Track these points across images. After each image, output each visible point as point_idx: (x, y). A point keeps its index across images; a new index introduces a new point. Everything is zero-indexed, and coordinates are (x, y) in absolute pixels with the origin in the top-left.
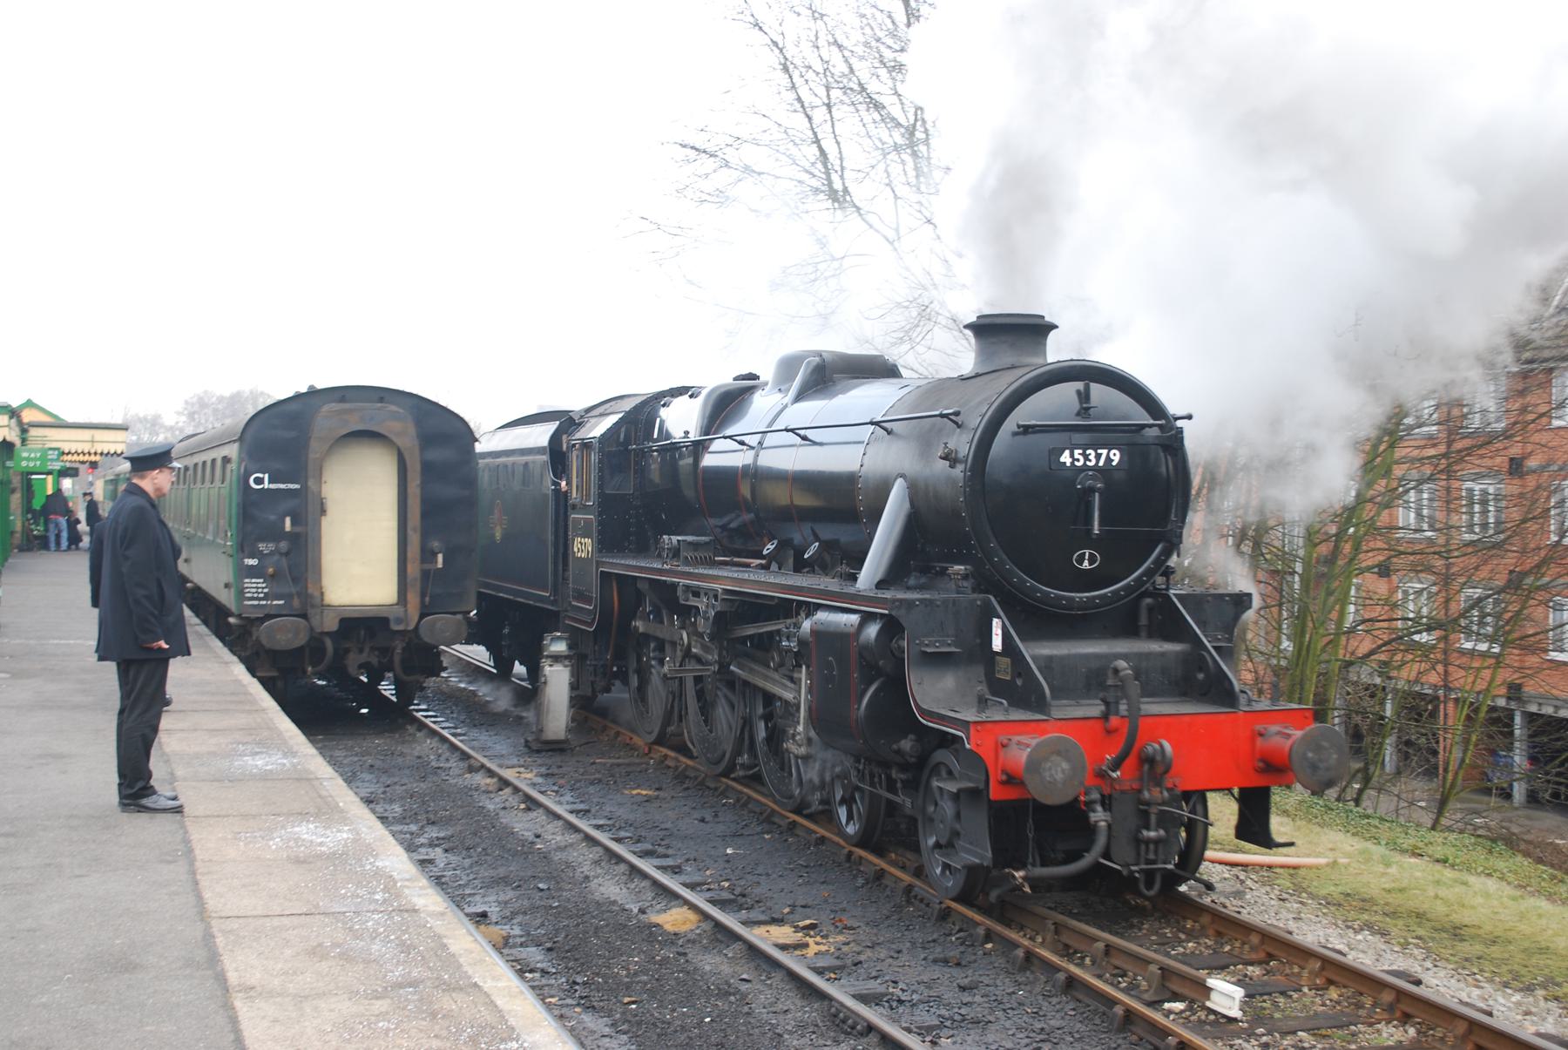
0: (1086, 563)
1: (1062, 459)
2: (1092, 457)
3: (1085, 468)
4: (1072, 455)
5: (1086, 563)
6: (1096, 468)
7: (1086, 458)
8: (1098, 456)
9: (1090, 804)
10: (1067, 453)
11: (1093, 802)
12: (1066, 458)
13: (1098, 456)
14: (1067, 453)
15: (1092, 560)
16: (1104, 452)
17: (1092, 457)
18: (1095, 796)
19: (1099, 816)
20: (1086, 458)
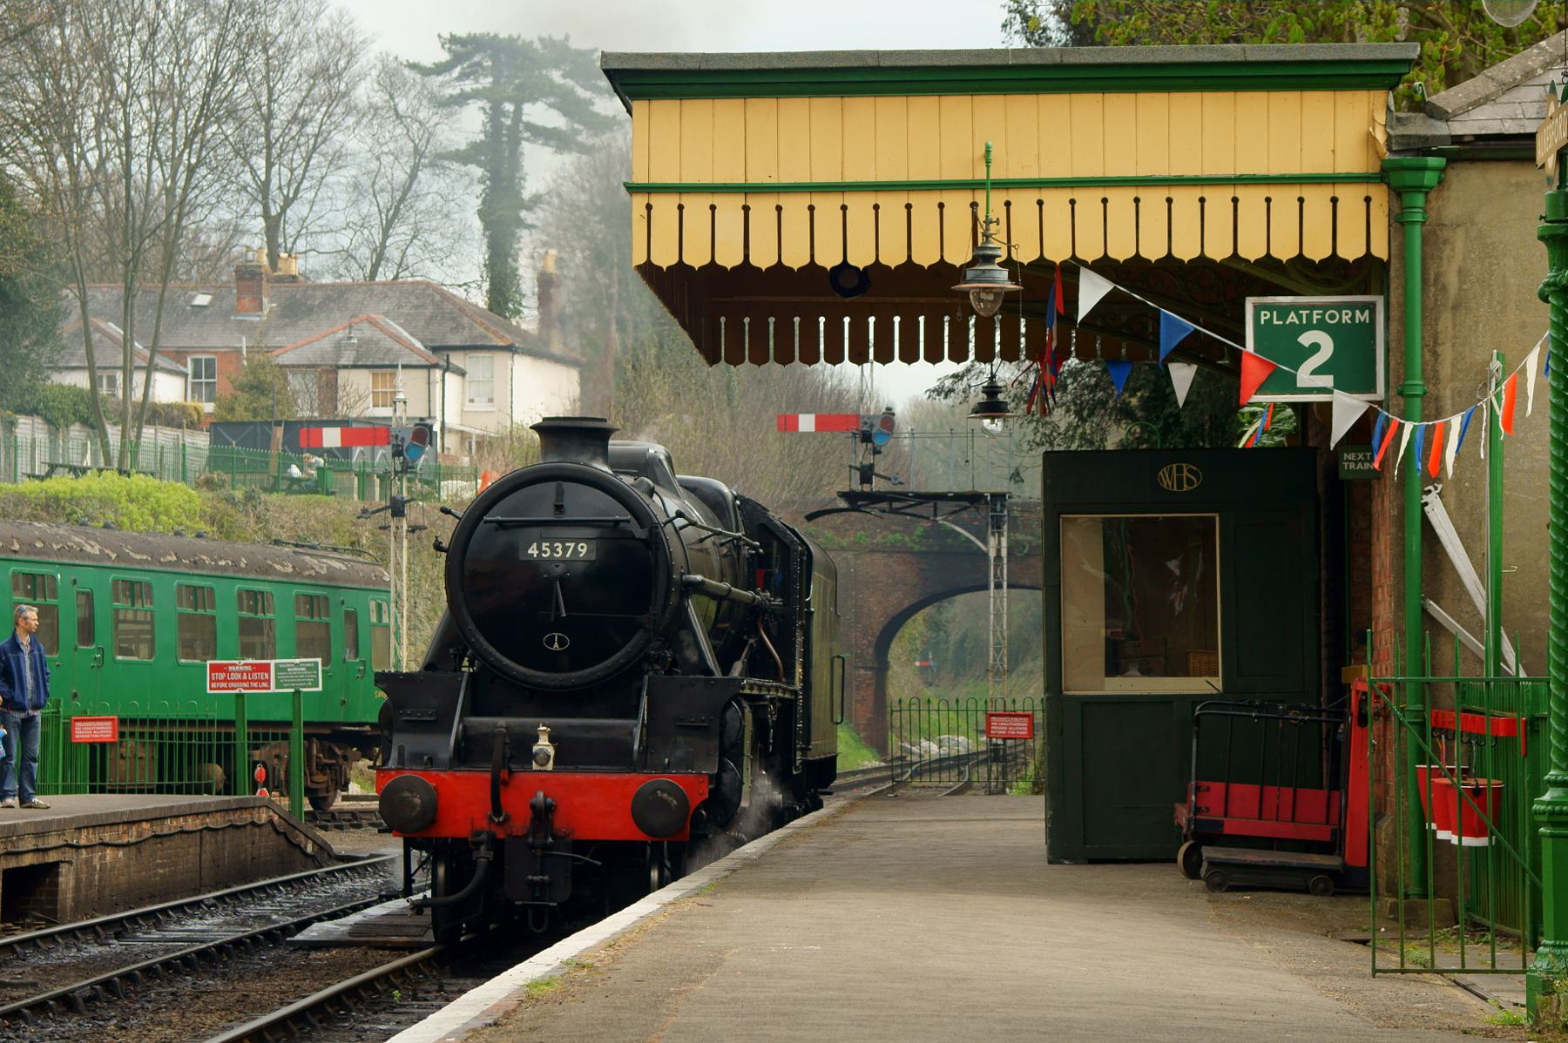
0: (556, 645)
1: (530, 551)
2: (559, 550)
3: (551, 560)
4: (539, 548)
5: (556, 645)
6: (563, 561)
7: (553, 550)
8: (565, 549)
9: (477, 845)
10: (535, 545)
11: (481, 843)
12: (533, 551)
13: (565, 549)
14: (535, 545)
15: (562, 642)
16: (572, 545)
17: (559, 550)
18: (483, 837)
19: (484, 855)
20: (553, 550)
